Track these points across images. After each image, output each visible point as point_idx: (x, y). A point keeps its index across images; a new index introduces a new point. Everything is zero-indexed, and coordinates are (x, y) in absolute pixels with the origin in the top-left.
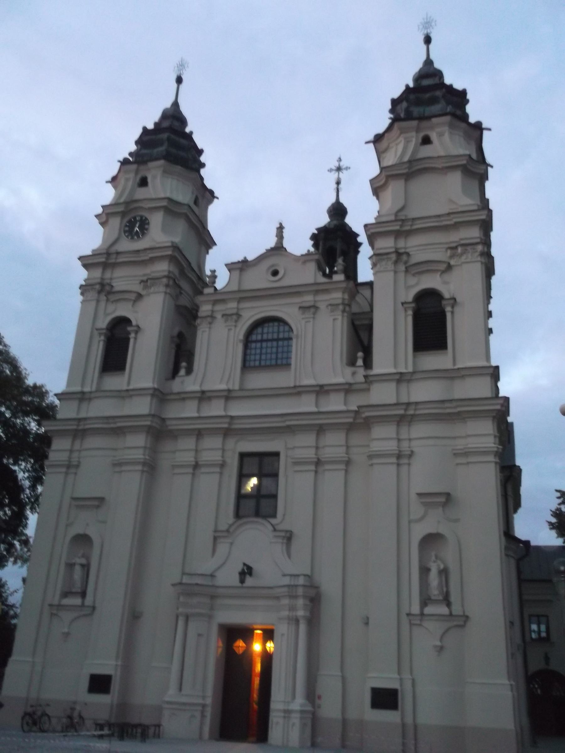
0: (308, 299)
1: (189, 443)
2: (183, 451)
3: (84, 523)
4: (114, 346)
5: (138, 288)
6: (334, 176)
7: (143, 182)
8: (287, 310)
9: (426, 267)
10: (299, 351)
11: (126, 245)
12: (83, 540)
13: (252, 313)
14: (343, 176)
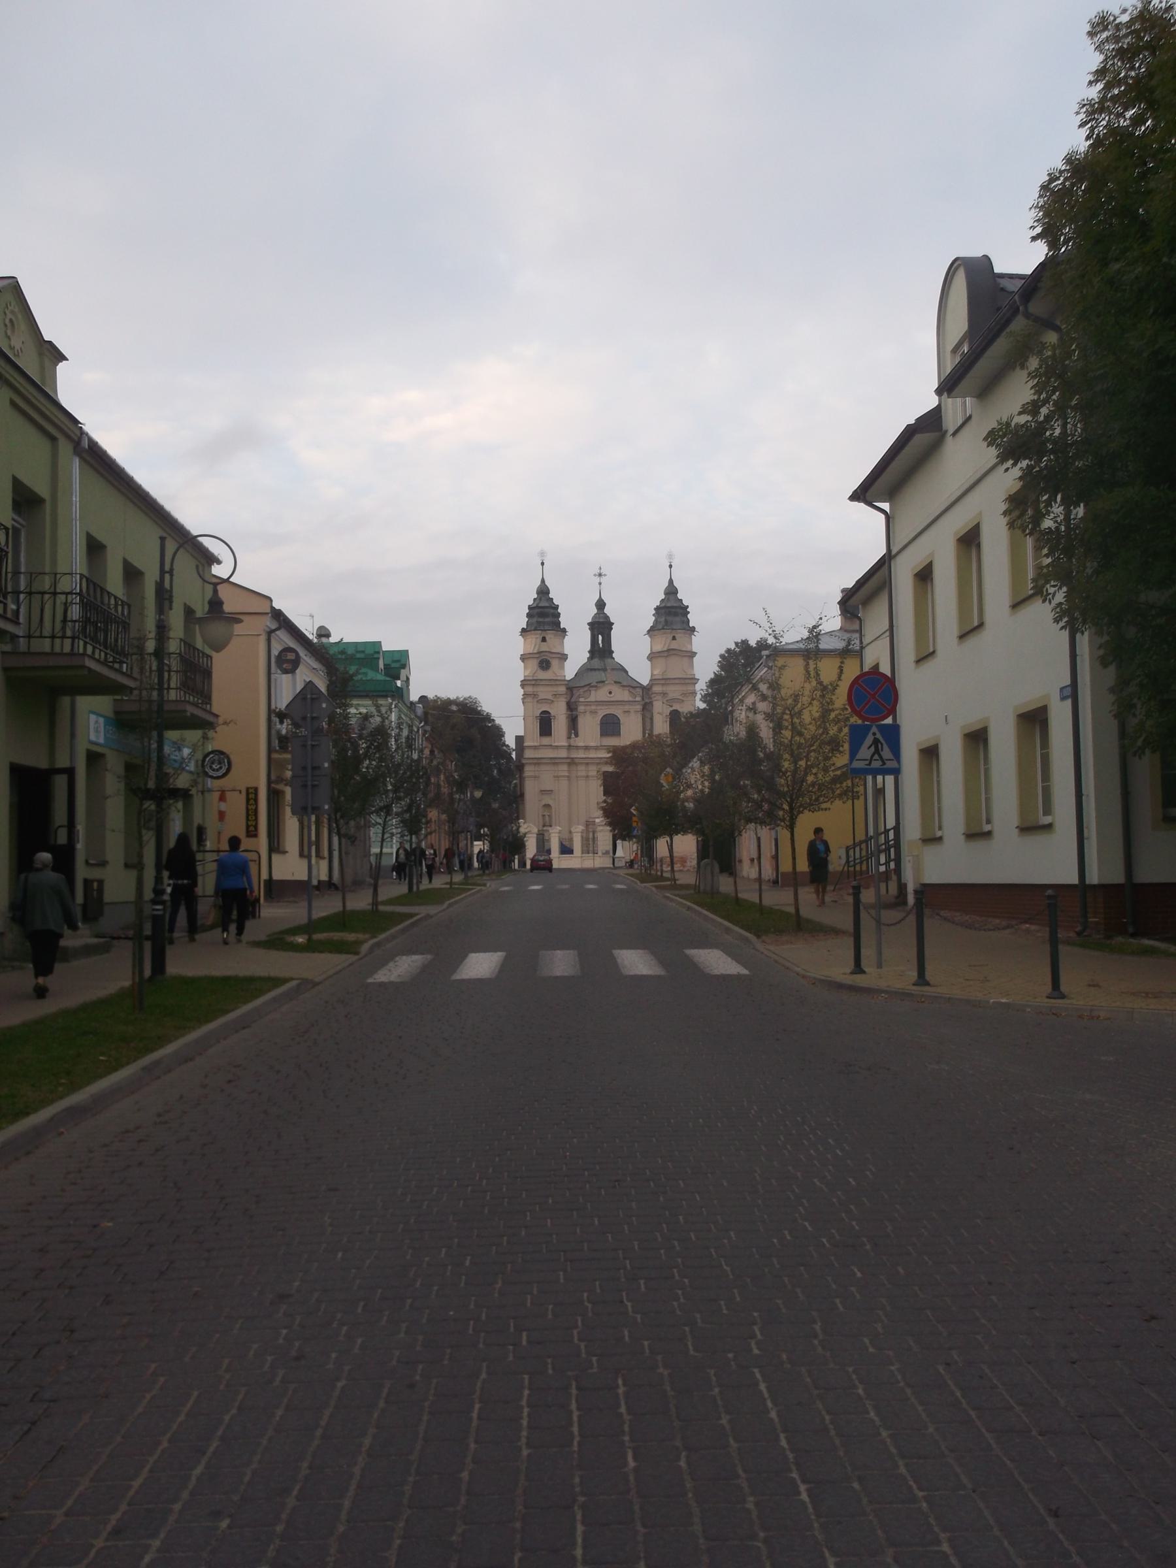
0: (627, 708)
1: (582, 768)
2: (581, 771)
3: (547, 800)
4: (545, 725)
5: (550, 697)
6: (597, 579)
7: (544, 640)
8: (617, 711)
9: (674, 700)
10: (623, 729)
11: (543, 675)
12: (547, 806)
13: (603, 711)
14: (603, 579)
